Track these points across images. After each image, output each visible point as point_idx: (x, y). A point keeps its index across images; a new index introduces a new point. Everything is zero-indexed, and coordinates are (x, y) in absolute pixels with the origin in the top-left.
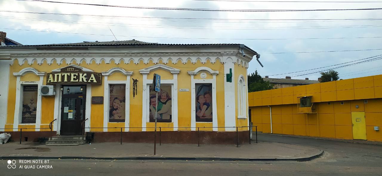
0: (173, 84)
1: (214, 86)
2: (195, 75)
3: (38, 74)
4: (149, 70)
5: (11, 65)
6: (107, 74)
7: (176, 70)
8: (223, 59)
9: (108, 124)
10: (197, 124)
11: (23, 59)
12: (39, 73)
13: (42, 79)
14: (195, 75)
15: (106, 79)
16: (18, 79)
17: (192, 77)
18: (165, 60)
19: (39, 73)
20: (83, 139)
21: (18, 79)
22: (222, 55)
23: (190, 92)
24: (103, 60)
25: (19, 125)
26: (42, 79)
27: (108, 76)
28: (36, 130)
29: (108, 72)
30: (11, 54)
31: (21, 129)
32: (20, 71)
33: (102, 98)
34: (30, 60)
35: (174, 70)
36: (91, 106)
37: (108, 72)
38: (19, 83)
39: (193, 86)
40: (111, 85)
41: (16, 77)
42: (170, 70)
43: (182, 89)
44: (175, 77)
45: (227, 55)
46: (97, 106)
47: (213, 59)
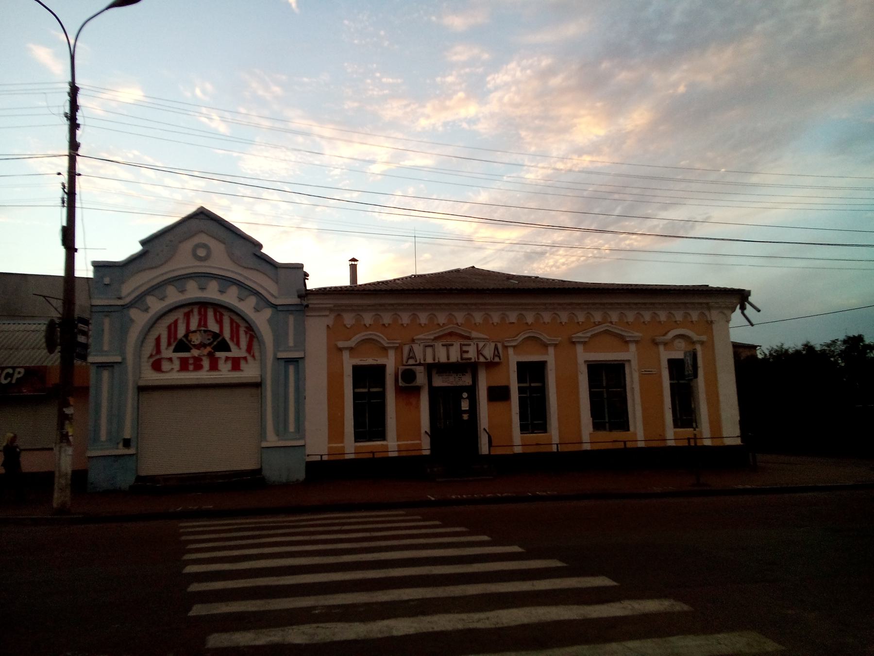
0: (629, 361)
2: (665, 344)
3: (386, 345)
4: (589, 335)
5: (330, 326)
6: (514, 344)
7: (636, 334)
8: (714, 315)
9: (522, 439)
10: (675, 433)
11: (353, 315)
12: (388, 343)
13: (392, 353)
14: (665, 344)
15: (511, 351)
16: (346, 355)
17: (661, 348)
18: (614, 316)
19: (388, 343)
21: (580, 349)
22: (709, 308)
23: (660, 376)
24: (521, 317)
26: (392, 353)
27: (514, 347)
28: (391, 454)
30: (334, 306)
32: (353, 339)
34: (368, 318)
35: (633, 335)
36: (488, 404)
38: (348, 363)
39: (664, 364)
41: (340, 350)
42: (623, 333)
44: (633, 347)
45: (720, 307)
47: (695, 315)
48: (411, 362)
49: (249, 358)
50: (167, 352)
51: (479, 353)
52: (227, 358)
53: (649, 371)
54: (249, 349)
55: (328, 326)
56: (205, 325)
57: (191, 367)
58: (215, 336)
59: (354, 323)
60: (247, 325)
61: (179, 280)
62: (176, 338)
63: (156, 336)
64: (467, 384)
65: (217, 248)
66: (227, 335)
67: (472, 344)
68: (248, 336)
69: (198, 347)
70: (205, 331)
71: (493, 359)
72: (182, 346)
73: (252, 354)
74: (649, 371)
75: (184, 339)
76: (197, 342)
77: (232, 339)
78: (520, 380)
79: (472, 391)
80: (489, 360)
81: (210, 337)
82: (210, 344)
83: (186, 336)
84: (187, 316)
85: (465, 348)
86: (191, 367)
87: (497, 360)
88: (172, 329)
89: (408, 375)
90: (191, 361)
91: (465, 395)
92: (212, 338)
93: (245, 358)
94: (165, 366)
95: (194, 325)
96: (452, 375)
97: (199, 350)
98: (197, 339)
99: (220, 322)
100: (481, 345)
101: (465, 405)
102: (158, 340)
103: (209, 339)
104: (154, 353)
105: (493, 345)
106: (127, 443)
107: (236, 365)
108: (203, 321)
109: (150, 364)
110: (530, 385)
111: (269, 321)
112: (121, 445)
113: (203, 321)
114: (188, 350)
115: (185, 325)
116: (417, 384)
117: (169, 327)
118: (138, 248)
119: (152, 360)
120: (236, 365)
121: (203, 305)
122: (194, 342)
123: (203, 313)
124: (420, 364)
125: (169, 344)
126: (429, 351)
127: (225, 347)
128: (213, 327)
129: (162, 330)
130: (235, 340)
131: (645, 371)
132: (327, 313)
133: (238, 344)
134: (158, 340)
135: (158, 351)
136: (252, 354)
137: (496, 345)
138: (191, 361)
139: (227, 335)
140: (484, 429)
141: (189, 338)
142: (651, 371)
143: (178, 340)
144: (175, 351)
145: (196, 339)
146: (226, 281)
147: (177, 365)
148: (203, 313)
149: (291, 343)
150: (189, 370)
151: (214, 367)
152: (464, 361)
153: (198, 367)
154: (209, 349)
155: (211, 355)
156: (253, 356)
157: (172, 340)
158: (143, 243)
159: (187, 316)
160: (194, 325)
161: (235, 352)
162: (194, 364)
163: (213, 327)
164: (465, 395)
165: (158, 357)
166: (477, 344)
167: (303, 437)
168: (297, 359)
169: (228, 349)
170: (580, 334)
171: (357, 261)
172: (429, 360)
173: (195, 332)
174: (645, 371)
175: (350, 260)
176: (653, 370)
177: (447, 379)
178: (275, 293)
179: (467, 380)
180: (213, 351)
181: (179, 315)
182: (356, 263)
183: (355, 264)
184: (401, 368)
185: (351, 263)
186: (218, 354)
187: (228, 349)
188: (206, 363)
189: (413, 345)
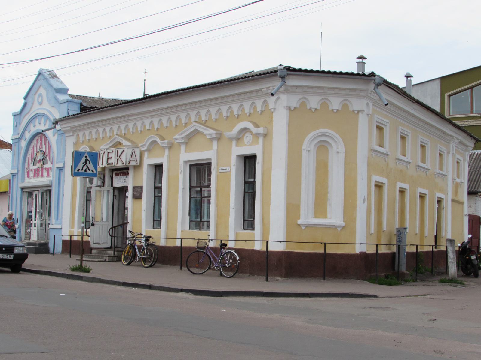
1: (259, 159)
25: (70, 231)
29: (145, 145)
31: (71, 236)
37: (145, 145)
39: (234, 160)
43: (223, 168)
46: (138, 201)
53: (225, 169)
55: (74, 143)
59: (84, 139)
62: (33, 157)
70: (42, 151)
71: (129, 163)
74: (225, 169)
85: (110, 155)
96: (121, 178)
132: (71, 134)
142: (226, 169)
152: (109, 166)
166: (118, 151)
168: (62, 168)
170: (177, 136)
174: (222, 169)
175: (358, 58)
176: (227, 168)
182: (364, 61)
183: (362, 62)
185: (358, 60)
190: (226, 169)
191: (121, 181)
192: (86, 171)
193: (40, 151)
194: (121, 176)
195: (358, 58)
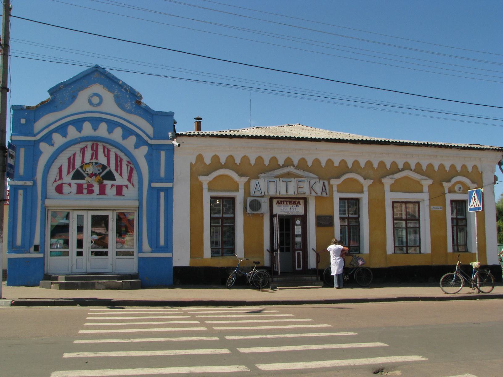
20: (317, 279)
33: (331, 218)
40: (341, 199)
43: (435, 207)
48: (258, 194)
49: (130, 185)
50: (67, 178)
51: (311, 188)
52: (112, 186)
53: (437, 208)
54: (129, 179)
56: (96, 158)
57: (85, 191)
58: (104, 167)
60: (129, 160)
61: (78, 124)
62: (74, 168)
63: (59, 166)
64: (300, 214)
65: (109, 98)
66: (112, 167)
67: (306, 181)
68: (129, 168)
69: (91, 175)
70: (96, 163)
72: (78, 175)
73: (132, 183)
74: (437, 208)
75: (80, 169)
76: (90, 172)
77: (116, 170)
78: (342, 212)
79: (304, 218)
80: (319, 195)
81: (100, 168)
82: (100, 174)
83: (82, 167)
84: (83, 150)
86: (85, 191)
87: (324, 194)
88: (71, 160)
89: (256, 205)
90: (85, 186)
91: (298, 222)
92: (101, 169)
93: (126, 186)
94: (66, 189)
95: (87, 159)
96: (288, 206)
97: (92, 178)
98: (90, 170)
99: (108, 157)
100: (313, 182)
101: (298, 230)
102: (60, 169)
103: (99, 170)
104: (58, 179)
105: (322, 182)
106: (37, 248)
107: (119, 190)
108: (95, 155)
109: (54, 188)
110: (348, 216)
111: (146, 157)
112: (32, 249)
113: (95, 155)
114: (83, 178)
115: (81, 158)
116: (262, 212)
117: (69, 159)
118: (47, 96)
119: (56, 184)
120: (119, 190)
121: (96, 141)
122: (87, 172)
123: (95, 149)
124: (262, 197)
125: (69, 172)
126: (272, 185)
127: (110, 176)
128: (102, 160)
129: (63, 160)
130: (119, 171)
131: (434, 208)
133: (121, 174)
134: (60, 169)
135: (61, 178)
136: (132, 183)
137: (324, 183)
138: (85, 186)
139: (112, 167)
140: (313, 249)
141: (84, 169)
142: (439, 208)
143: (75, 170)
144: (74, 178)
145: (90, 170)
146: (112, 125)
147: (74, 189)
148: (95, 149)
149: (162, 174)
150: (83, 194)
151: (102, 191)
153: (90, 192)
154: (99, 177)
155: (100, 183)
156: (133, 185)
157: (71, 170)
158: (52, 91)
159: (83, 150)
160: (87, 159)
161: (120, 180)
162: (88, 189)
163: (102, 160)
164: (298, 222)
165: (60, 182)
167: (171, 252)
169: (113, 179)
171: (201, 119)
172: (272, 193)
173: (88, 164)
174: (434, 208)
177: (284, 209)
178: (152, 136)
179: (299, 210)
180: (101, 179)
181: (76, 148)
182: (200, 121)
184: (249, 199)
185: (196, 120)
186: (105, 182)
187: (113, 179)
188: (96, 188)
189: (259, 180)
190: (439, 208)
191: (292, 209)
192: (475, 206)
193: (92, 163)
194: (288, 205)
195: (195, 119)
